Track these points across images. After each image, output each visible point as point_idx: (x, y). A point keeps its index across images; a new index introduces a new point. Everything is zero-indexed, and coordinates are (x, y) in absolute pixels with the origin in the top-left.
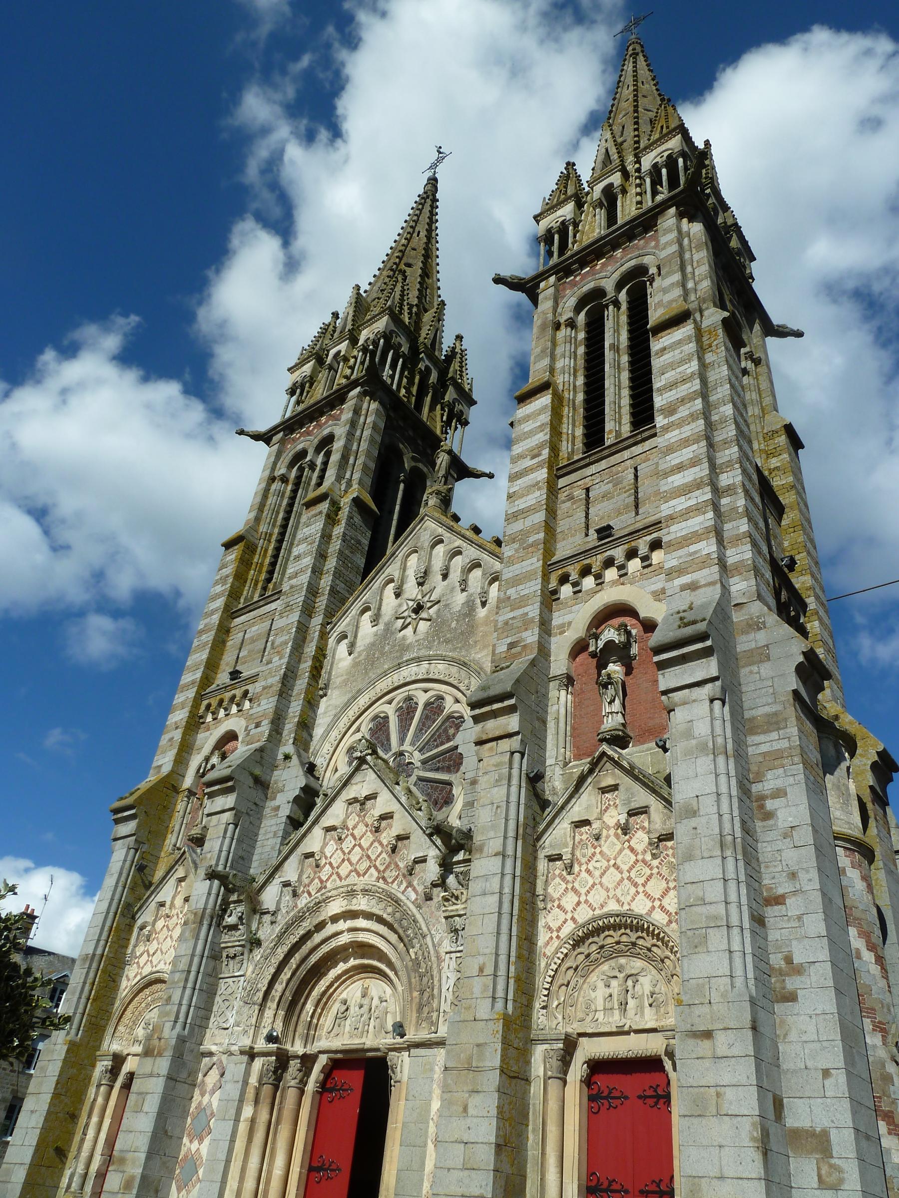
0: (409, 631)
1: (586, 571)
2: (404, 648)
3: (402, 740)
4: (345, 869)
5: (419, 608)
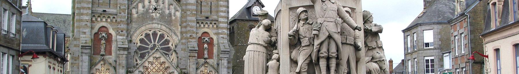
0: (154, 14)
1: (202, 23)
2: (153, 19)
3: (155, 41)
4: (154, 70)
5: (155, 9)
